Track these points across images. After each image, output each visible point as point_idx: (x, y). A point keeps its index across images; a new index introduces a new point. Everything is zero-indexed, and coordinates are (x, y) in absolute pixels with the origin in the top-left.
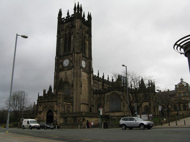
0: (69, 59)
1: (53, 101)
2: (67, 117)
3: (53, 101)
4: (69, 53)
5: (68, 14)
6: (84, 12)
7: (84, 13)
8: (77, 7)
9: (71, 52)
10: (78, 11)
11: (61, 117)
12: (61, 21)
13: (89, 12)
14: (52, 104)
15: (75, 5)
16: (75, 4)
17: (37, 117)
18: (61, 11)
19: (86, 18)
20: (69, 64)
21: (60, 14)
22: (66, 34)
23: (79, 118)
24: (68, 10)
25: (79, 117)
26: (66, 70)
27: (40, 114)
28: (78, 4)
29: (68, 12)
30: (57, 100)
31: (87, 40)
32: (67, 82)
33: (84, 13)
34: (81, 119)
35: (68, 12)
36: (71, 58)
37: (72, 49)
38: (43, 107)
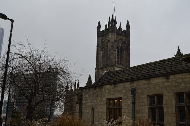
7: (120, 24)
10: (112, 25)
12: (100, 34)
15: (110, 19)
16: (110, 18)
18: (100, 23)
19: (124, 28)
21: (99, 26)
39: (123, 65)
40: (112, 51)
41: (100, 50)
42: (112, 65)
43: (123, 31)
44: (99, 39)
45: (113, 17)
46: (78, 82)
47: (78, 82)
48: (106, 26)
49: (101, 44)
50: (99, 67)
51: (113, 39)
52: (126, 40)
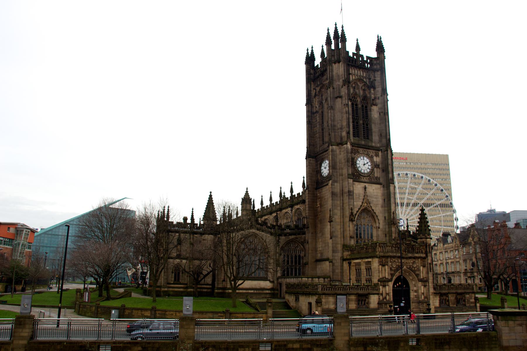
0: (371, 158)
1: (415, 258)
2: (446, 294)
3: (415, 258)
4: (370, 144)
5: (358, 48)
9: (373, 144)
11: (434, 293)
14: (414, 263)
17: (378, 294)
20: (372, 170)
23: (468, 296)
24: (357, 40)
25: (468, 293)
26: (365, 182)
27: (384, 286)
29: (357, 43)
30: (424, 255)
32: (371, 210)
34: (471, 298)
35: (357, 43)
36: (375, 159)
37: (375, 137)
38: (391, 269)
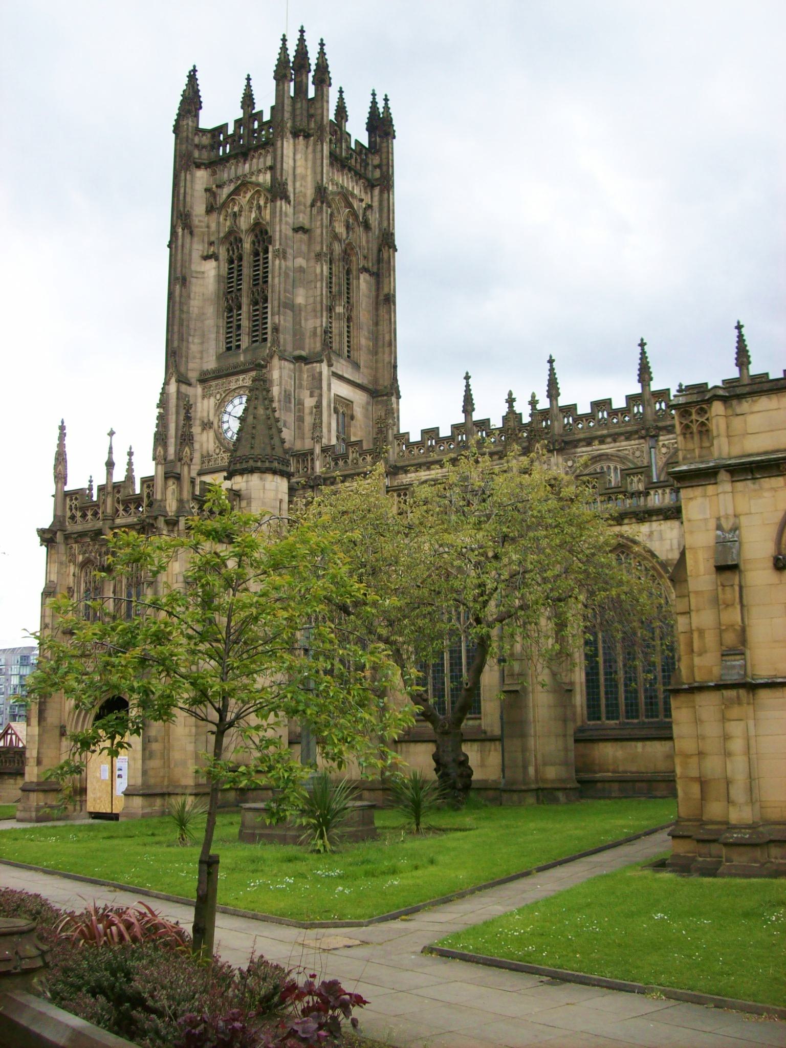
6: (341, 92)
7: (341, 99)
8: (292, 59)
13: (374, 95)
15: (284, 49)
16: (284, 40)
22: (232, 238)
28: (302, 40)
31: (365, 270)
33: (341, 99)
35: (248, 86)
39: (356, 366)
40: (301, 262)
41: (196, 255)
42: (303, 353)
43: (353, 146)
44: (193, 176)
45: (302, 40)
46: (130, 464)
47: (130, 464)
48: (248, 100)
49: (210, 210)
50: (191, 365)
51: (304, 178)
52: (369, 207)
